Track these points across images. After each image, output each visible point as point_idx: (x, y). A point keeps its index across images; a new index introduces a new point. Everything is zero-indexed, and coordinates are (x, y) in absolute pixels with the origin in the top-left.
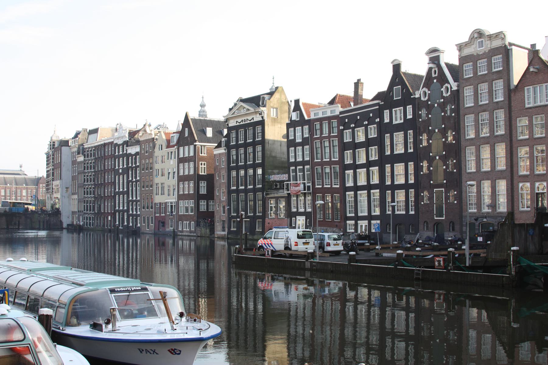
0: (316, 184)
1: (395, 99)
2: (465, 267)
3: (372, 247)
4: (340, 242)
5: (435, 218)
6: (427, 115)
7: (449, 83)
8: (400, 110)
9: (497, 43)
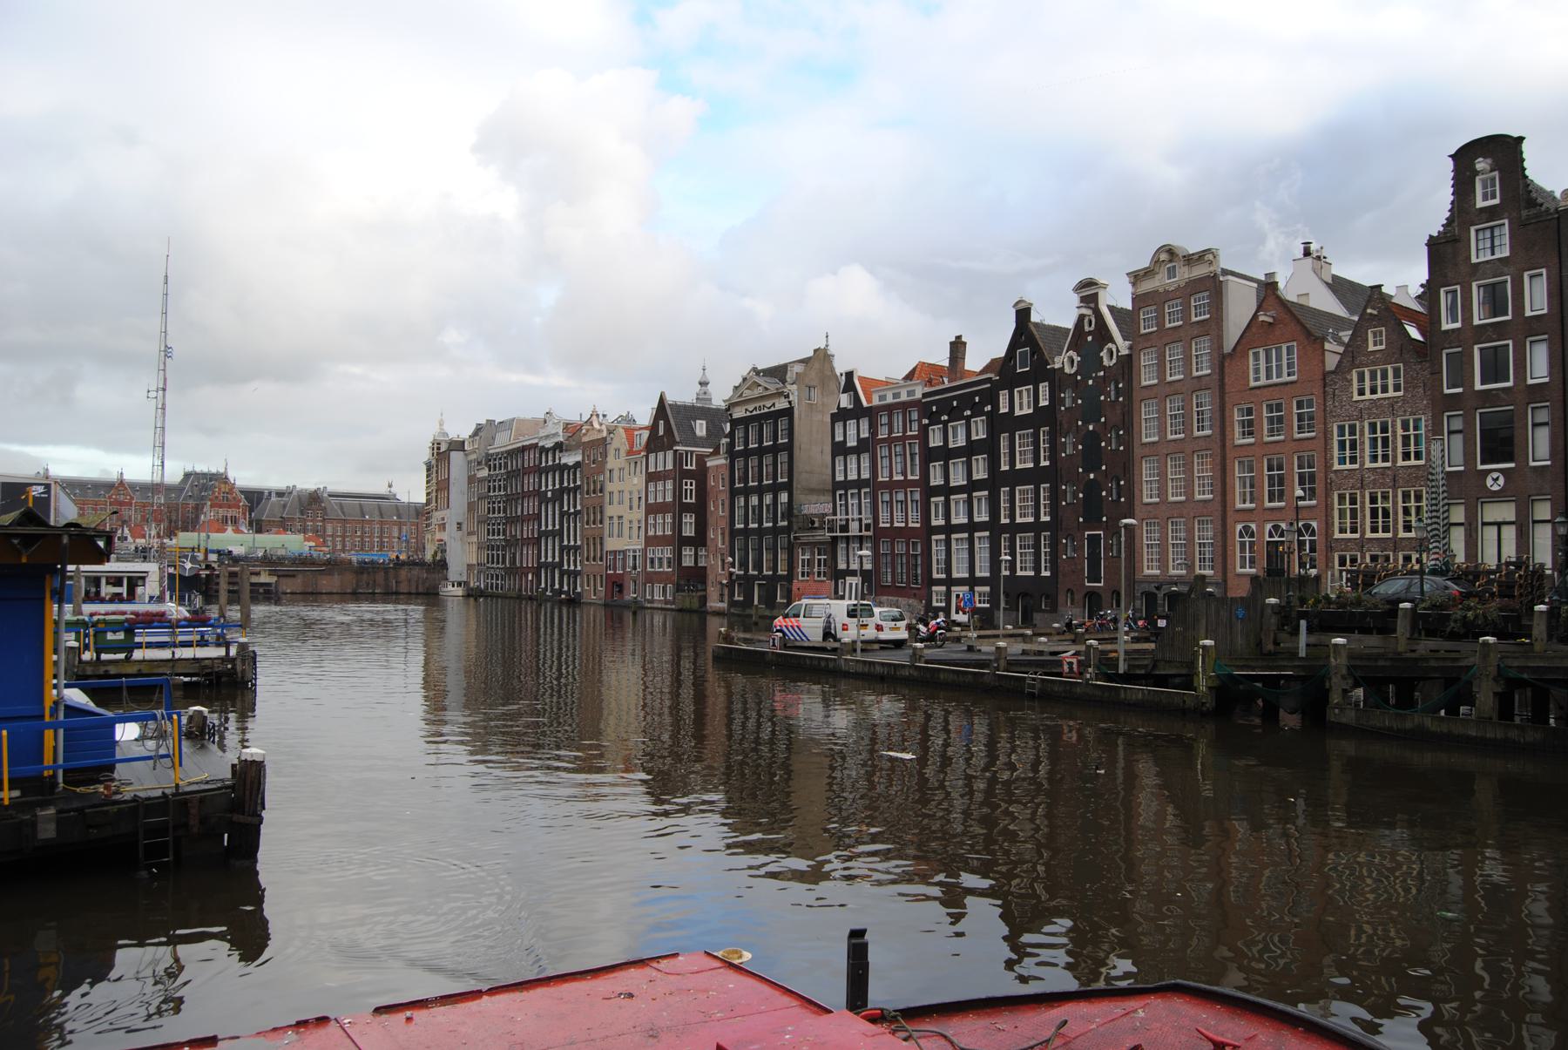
0: (881, 521)
1: (1018, 371)
2: (1117, 674)
3: (963, 634)
4: (903, 624)
5: (1087, 584)
6: (1074, 400)
7: (1113, 342)
8: (1028, 390)
9: (1200, 271)
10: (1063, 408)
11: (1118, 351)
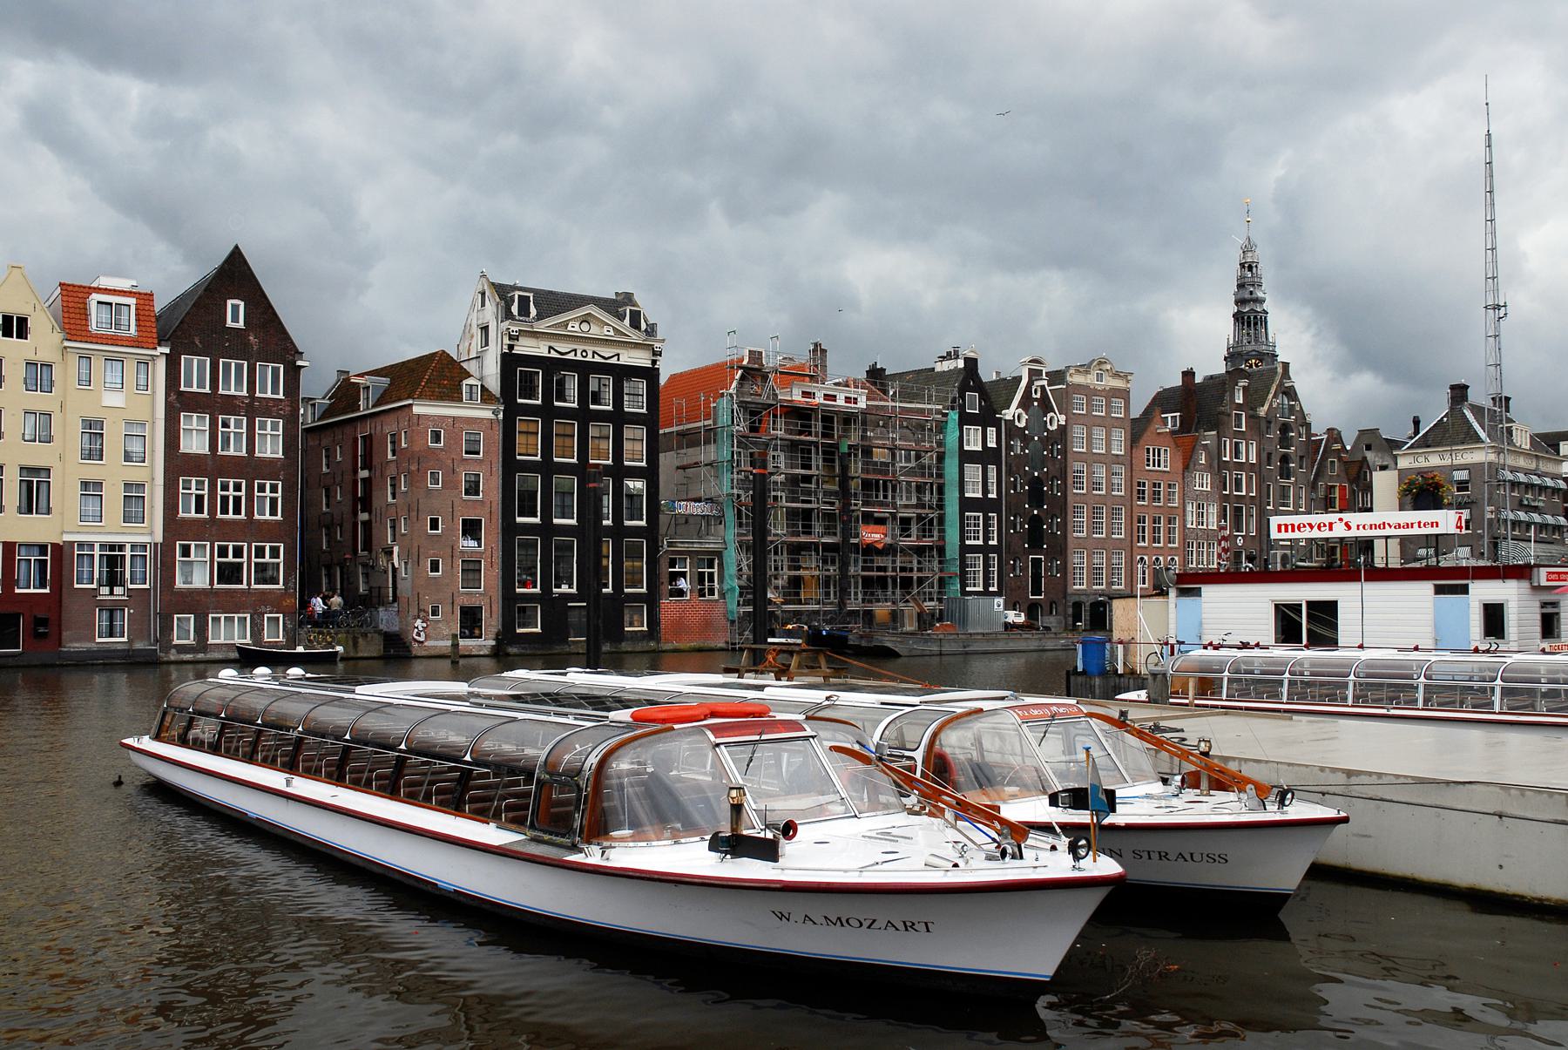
6: (1023, 449)
10: (1012, 453)
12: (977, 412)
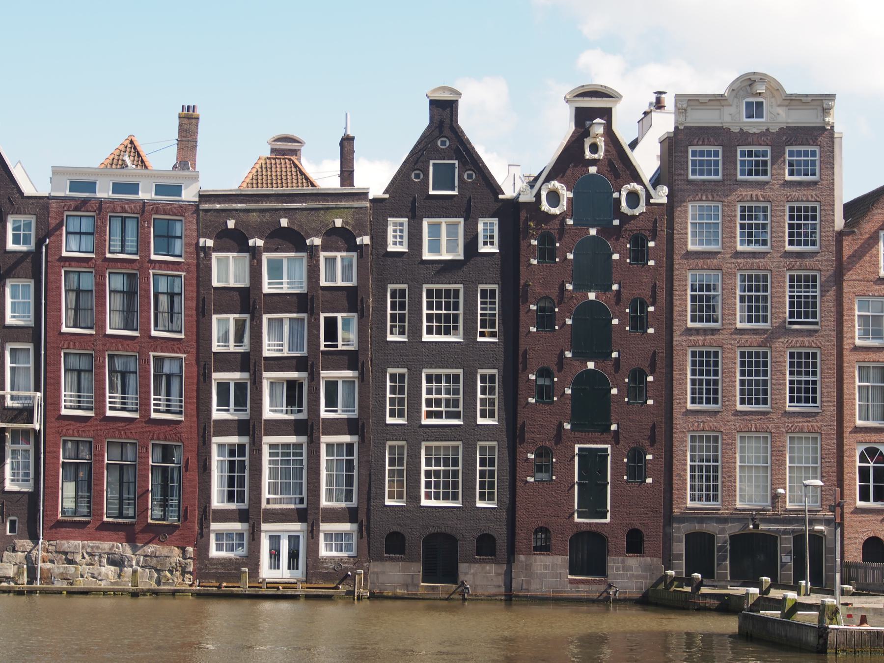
5: (577, 519)
11: (649, 196)
12: (455, 193)
